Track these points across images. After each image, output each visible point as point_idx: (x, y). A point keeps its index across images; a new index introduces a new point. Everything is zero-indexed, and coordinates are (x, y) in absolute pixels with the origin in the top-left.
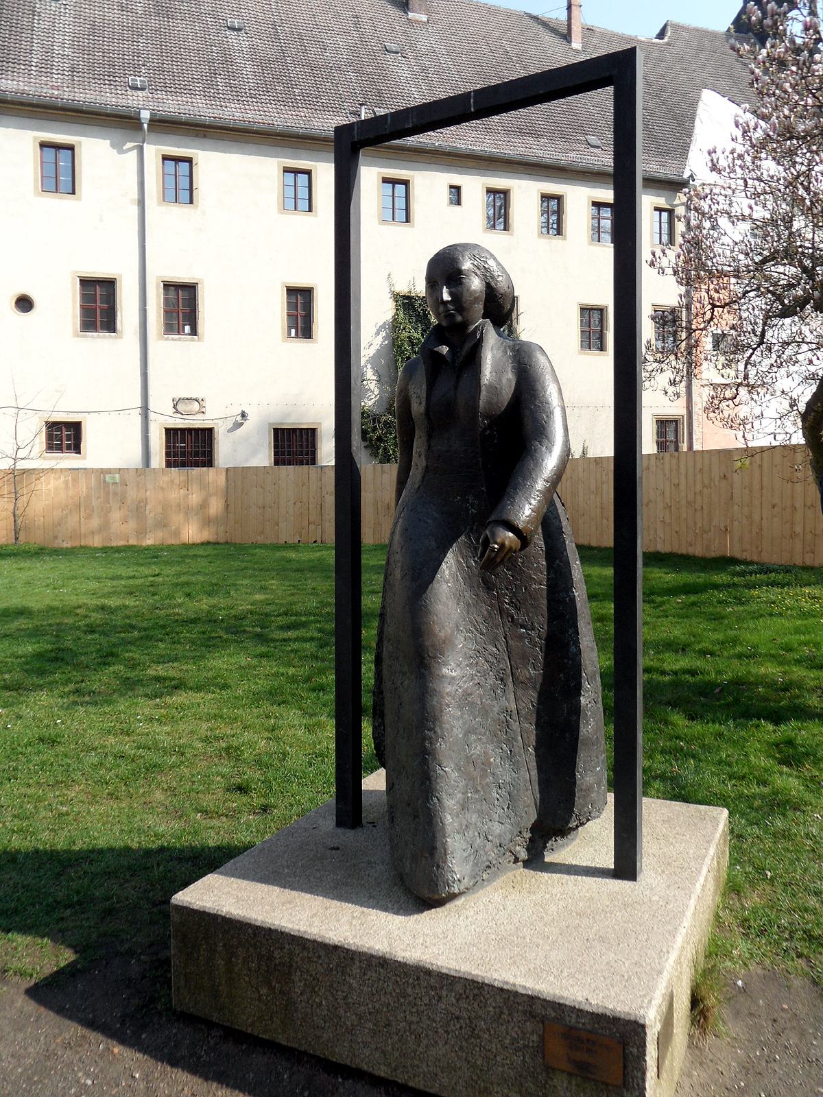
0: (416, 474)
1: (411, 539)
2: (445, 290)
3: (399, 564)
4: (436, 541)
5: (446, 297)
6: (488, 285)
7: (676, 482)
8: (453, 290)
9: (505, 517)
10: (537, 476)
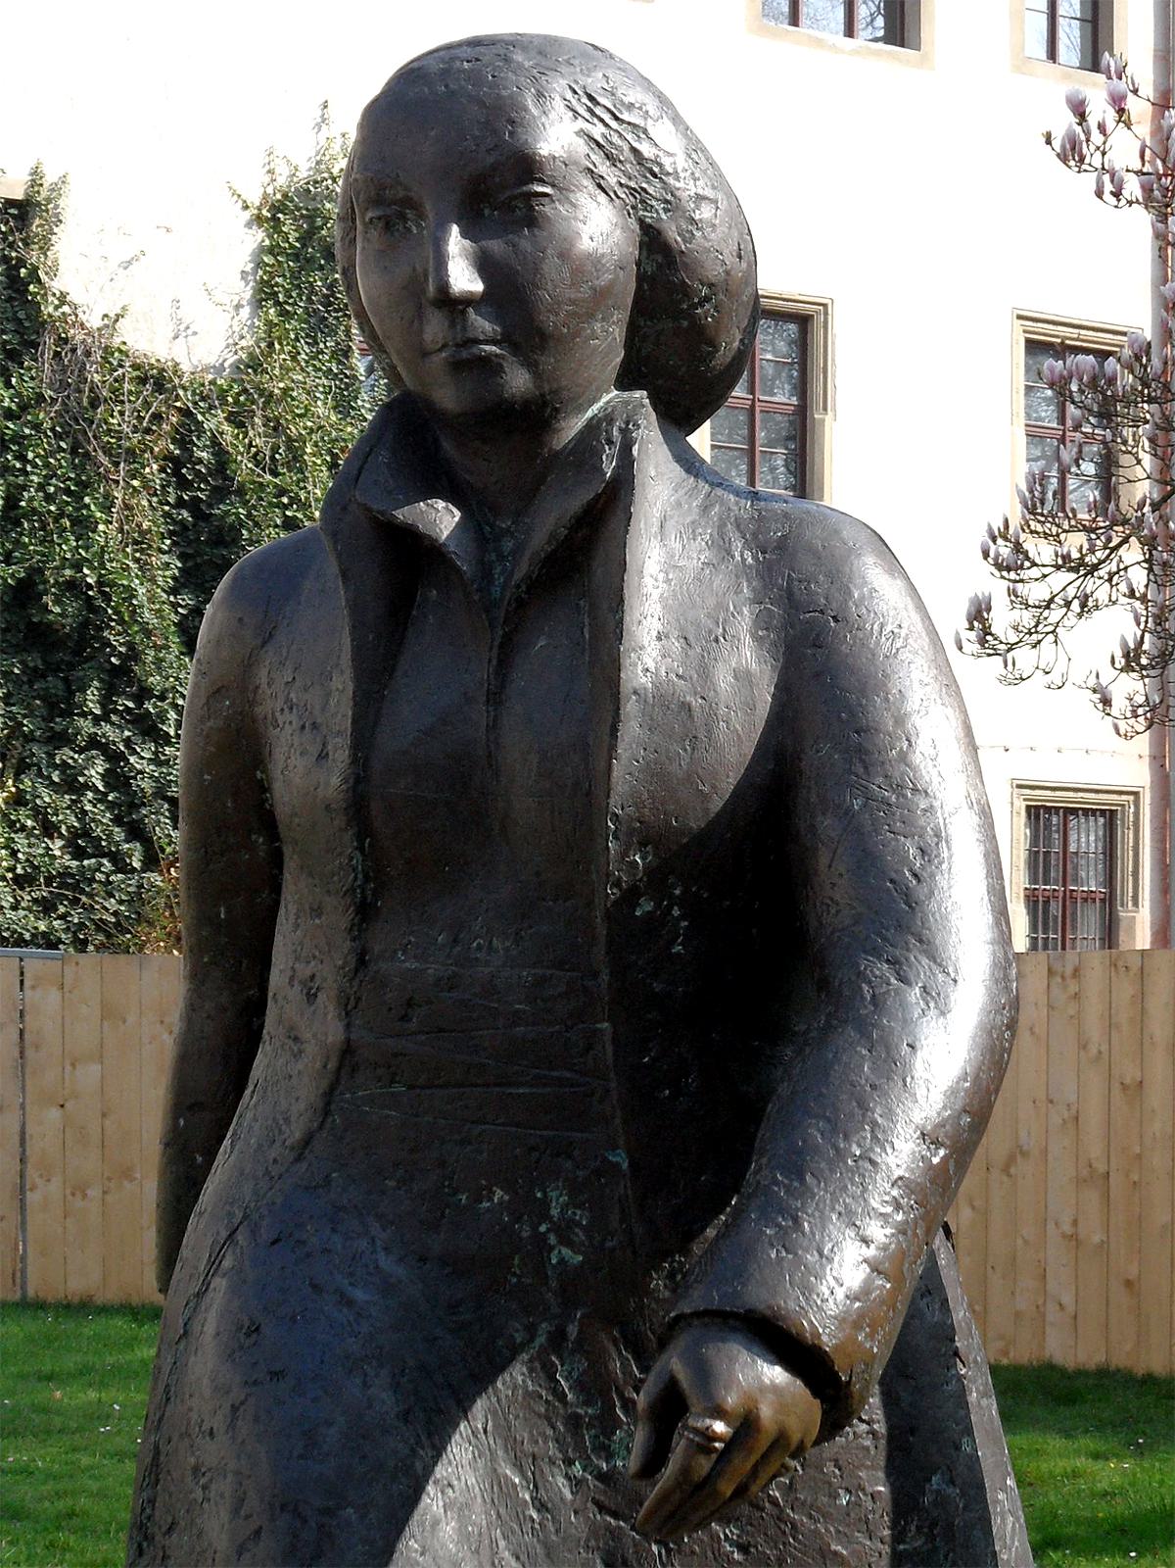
0: (285, 1079)
1: (276, 1375)
2: (456, 243)
3: (224, 1486)
4: (396, 1387)
5: (464, 278)
6: (651, 240)
7: (1131, 1074)
8: (496, 246)
9: (756, 1297)
10: (890, 1115)
